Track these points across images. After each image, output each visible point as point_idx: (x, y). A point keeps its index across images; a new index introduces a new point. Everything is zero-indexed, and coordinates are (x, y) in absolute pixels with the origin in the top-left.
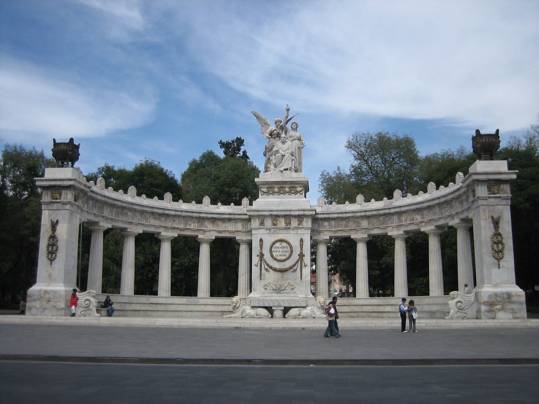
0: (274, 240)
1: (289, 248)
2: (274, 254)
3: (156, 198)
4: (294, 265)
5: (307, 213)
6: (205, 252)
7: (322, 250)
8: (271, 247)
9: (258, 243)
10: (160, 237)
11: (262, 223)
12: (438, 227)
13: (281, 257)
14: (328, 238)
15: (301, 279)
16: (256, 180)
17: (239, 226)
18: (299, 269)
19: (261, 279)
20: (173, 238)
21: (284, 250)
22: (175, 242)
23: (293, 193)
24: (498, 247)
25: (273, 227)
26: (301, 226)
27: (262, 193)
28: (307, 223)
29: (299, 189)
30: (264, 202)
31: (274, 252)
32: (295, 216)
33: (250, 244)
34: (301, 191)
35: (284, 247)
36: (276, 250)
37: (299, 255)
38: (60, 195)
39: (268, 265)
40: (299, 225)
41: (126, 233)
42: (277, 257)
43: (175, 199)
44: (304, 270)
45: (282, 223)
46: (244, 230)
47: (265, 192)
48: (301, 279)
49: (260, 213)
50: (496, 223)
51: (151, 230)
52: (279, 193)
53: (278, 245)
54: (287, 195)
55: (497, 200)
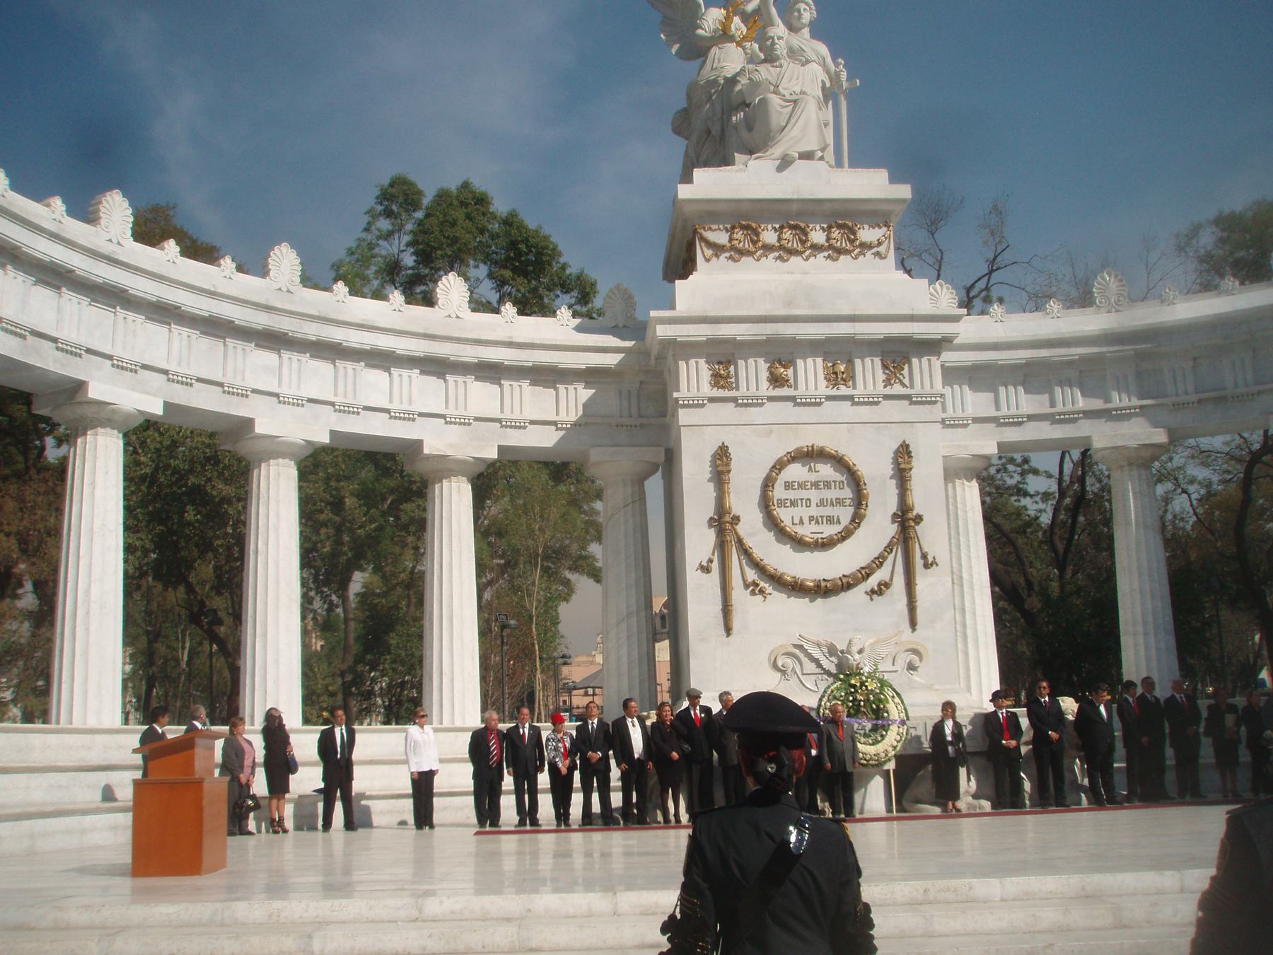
0: (780, 453)
2: (785, 516)
6: (454, 509)
11: (719, 380)
13: (815, 528)
14: (991, 449)
15: (913, 624)
16: (684, 192)
18: (899, 582)
19: (728, 630)
21: (832, 494)
26: (897, 389)
27: (709, 252)
31: (782, 503)
35: (828, 485)
36: (791, 495)
40: (888, 383)
44: (923, 581)
45: (810, 374)
48: (913, 624)
53: (796, 472)
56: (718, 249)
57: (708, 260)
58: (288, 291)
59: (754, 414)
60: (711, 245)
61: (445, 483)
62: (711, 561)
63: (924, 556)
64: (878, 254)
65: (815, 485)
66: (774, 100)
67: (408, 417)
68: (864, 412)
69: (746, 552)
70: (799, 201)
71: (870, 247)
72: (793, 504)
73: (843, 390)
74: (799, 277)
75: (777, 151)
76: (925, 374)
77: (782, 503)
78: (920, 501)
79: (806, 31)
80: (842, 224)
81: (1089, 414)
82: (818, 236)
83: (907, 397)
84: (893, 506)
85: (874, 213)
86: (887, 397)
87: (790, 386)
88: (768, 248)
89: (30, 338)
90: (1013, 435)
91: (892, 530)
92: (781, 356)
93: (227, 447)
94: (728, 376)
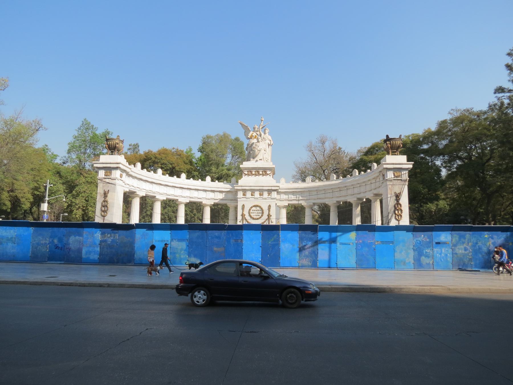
2: (252, 215)
3: (175, 177)
4: (265, 221)
5: (273, 188)
8: (250, 210)
9: (241, 208)
11: (244, 195)
12: (359, 199)
16: (241, 166)
22: (187, 205)
24: (398, 212)
30: (246, 181)
32: (266, 190)
33: (236, 208)
38: (111, 173)
39: (248, 222)
43: (188, 178)
45: (257, 194)
50: (398, 197)
53: (254, 208)
55: (399, 181)
56: (246, 174)
66: (256, 150)
69: (246, 220)
75: (256, 159)
76: (274, 195)
78: (271, 213)
79: (267, 134)
80: (264, 171)
81: (301, 200)
82: (261, 173)
85: (270, 169)
88: (253, 174)
91: (267, 217)
92: (253, 191)
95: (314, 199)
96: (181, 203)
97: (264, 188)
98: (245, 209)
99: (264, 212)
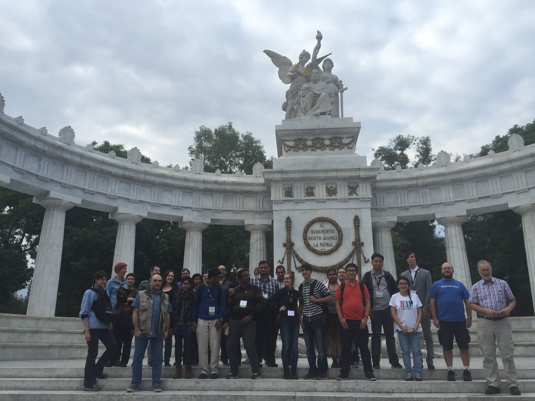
1: (336, 232)
2: (312, 243)
7: (386, 239)
8: (306, 232)
10: (117, 218)
17: (251, 204)
20: (140, 220)
23: (337, 147)
25: (307, 198)
27: (287, 149)
28: (364, 191)
29: (345, 141)
31: (311, 238)
34: (350, 143)
35: (327, 232)
36: (314, 235)
37: (354, 244)
39: (301, 261)
40: (350, 194)
41: (47, 202)
42: (316, 248)
46: (258, 209)
47: (291, 147)
49: (285, 176)
51: (99, 202)
52: (314, 147)
53: (316, 227)
54: (327, 150)
57: (287, 152)
58: (136, 163)
59: (300, 206)
60: (288, 146)
61: (192, 233)
62: (283, 260)
63: (365, 259)
64: (348, 148)
65: (323, 232)
67: (178, 208)
68: (342, 205)
70: (319, 129)
71: (346, 145)
72: (314, 239)
73: (334, 197)
74: (318, 157)
77: (311, 238)
83: (359, 199)
84: (352, 238)
86: (349, 199)
87: (314, 196)
89: (26, 175)
90: (404, 214)
93: (112, 218)
94: (291, 192)
95: (470, 201)
96: (128, 219)
97: (340, 174)
98: (293, 231)
99: (344, 233)
